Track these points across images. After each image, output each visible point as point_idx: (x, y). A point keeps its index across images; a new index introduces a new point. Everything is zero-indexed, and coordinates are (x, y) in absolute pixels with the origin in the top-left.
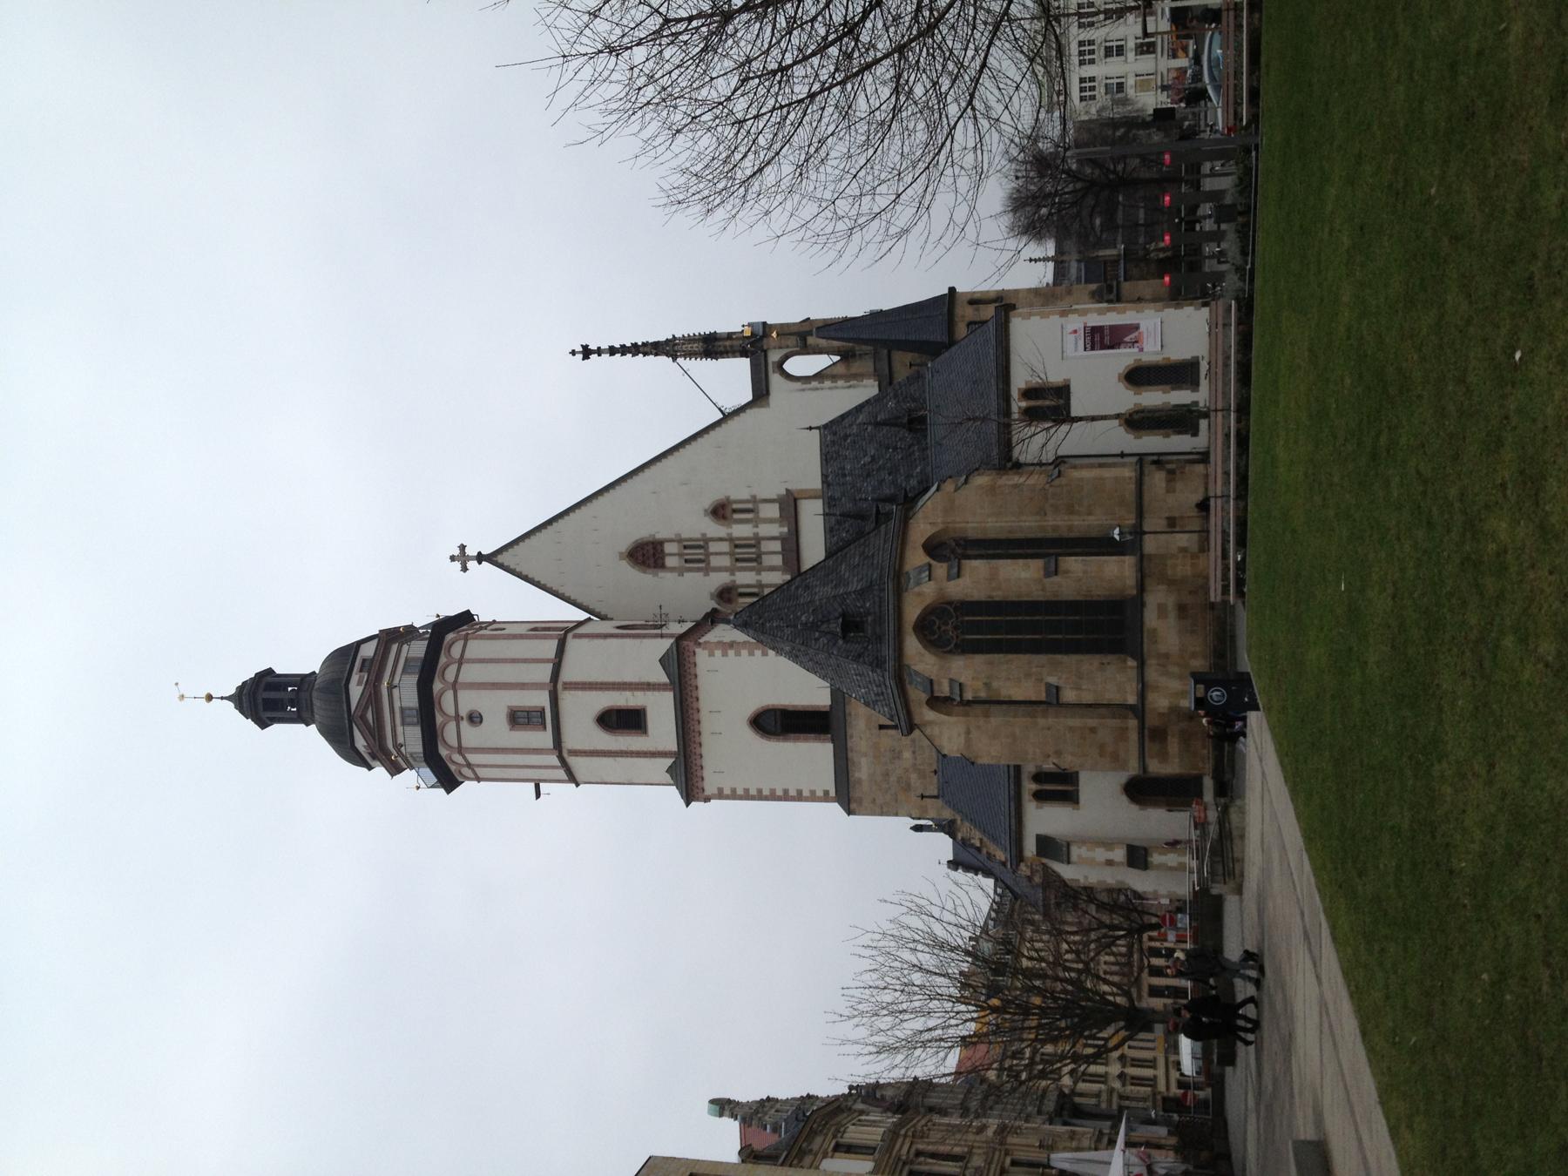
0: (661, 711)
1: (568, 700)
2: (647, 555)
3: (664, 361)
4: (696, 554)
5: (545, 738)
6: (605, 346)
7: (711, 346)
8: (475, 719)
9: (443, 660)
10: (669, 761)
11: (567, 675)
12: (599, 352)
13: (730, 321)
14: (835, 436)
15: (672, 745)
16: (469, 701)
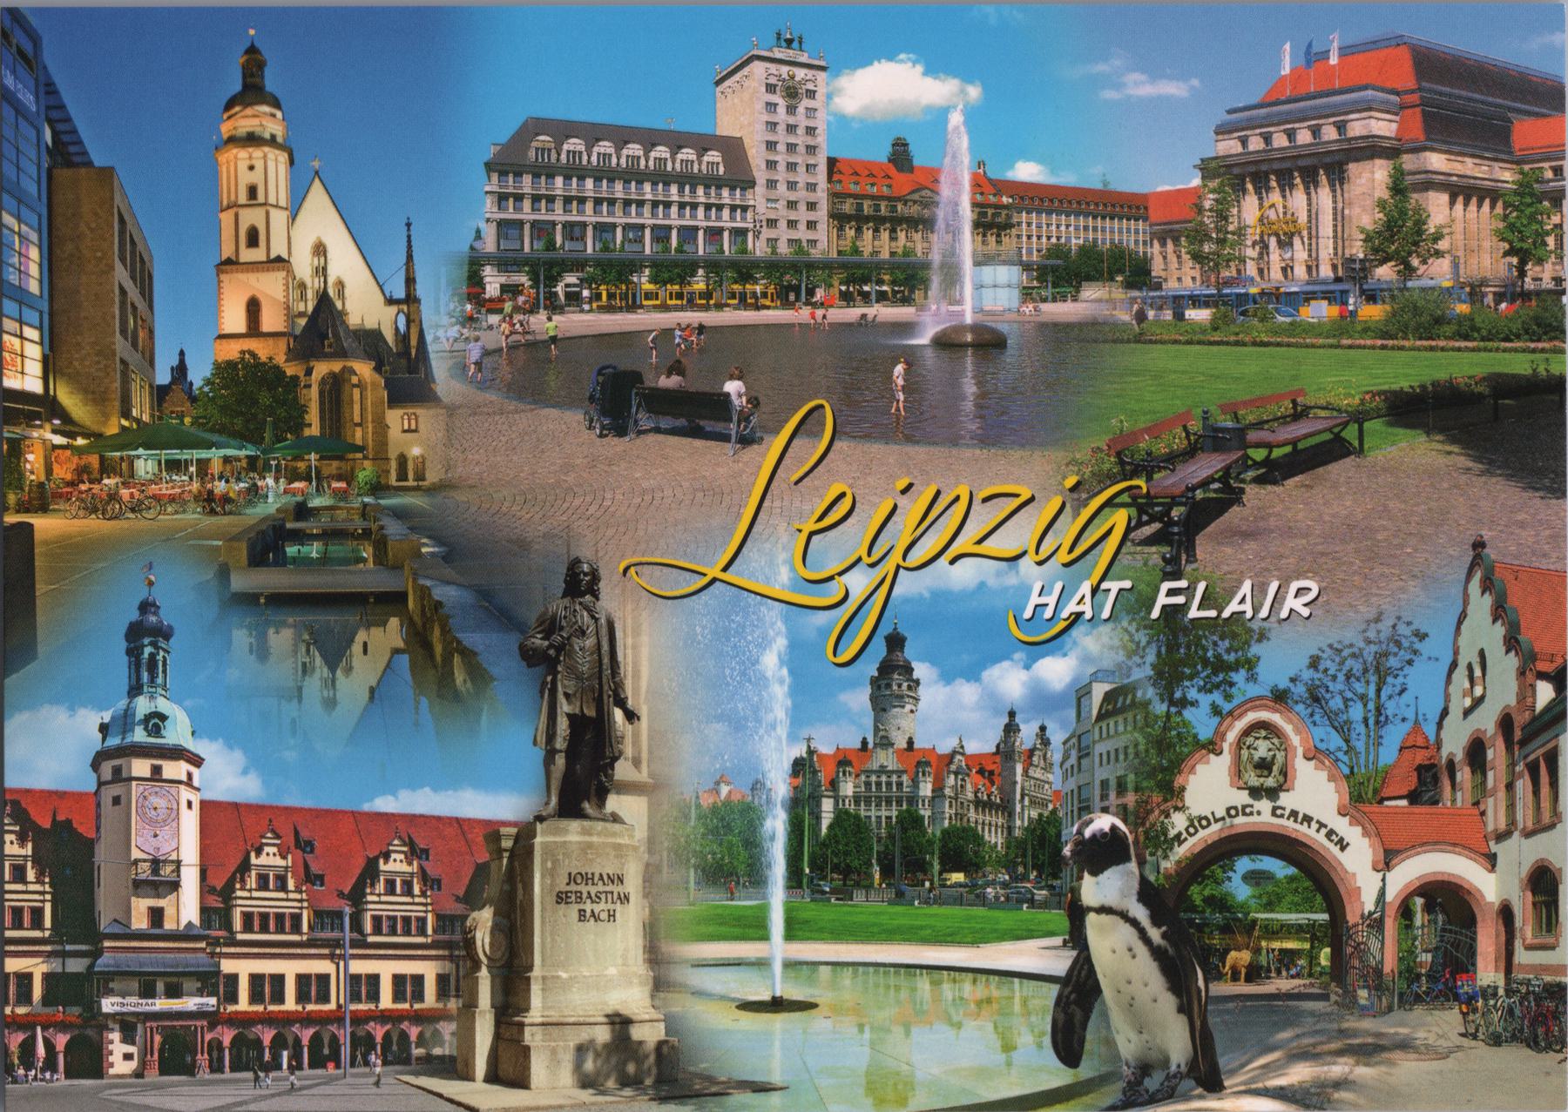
0: (258, 254)
1: (260, 212)
2: (320, 250)
3: (404, 261)
4: (322, 271)
5: (243, 199)
6: (412, 233)
7: (410, 281)
8: (251, 168)
9: (277, 152)
10: (234, 258)
11: (273, 212)
12: (409, 230)
13: (421, 290)
14: (376, 335)
15: (242, 260)
16: (259, 165)
